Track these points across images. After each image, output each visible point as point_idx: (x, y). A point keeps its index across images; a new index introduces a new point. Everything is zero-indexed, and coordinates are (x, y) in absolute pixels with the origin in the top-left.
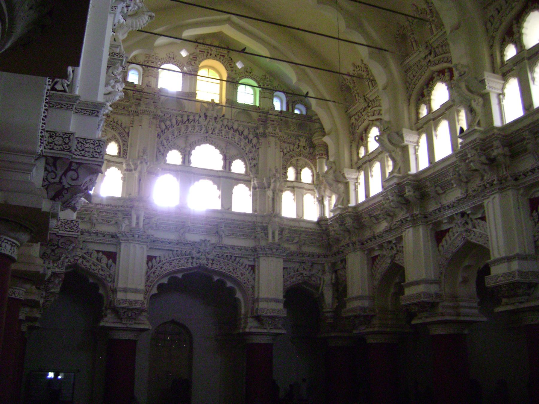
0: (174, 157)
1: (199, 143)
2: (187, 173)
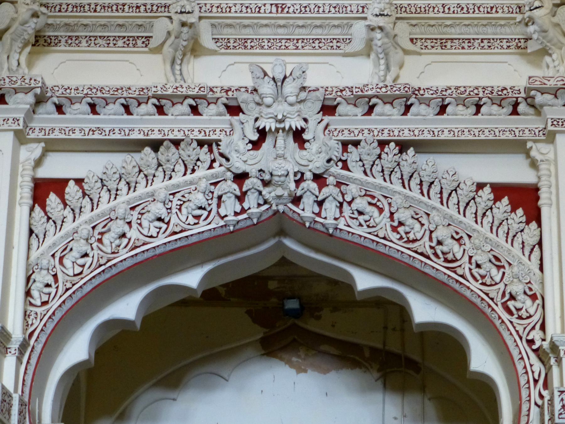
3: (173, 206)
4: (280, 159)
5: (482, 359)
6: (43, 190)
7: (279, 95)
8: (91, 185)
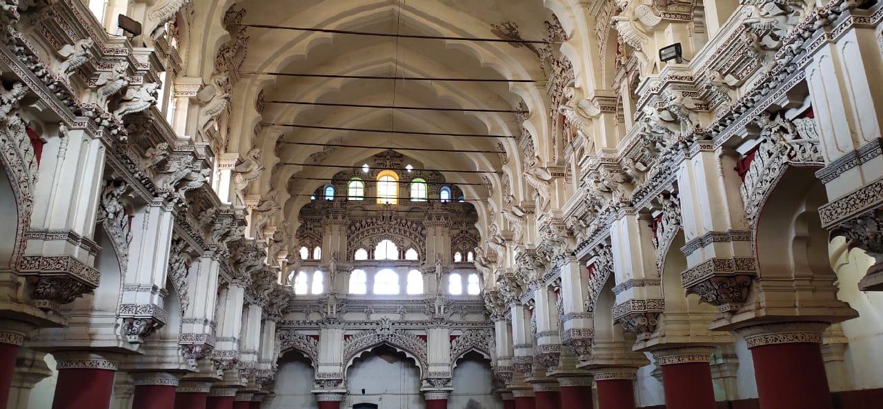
0: (361, 255)
2: (372, 265)
3: (369, 340)
4: (386, 332)
5: (417, 364)
6: (346, 337)
8: (354, 336)
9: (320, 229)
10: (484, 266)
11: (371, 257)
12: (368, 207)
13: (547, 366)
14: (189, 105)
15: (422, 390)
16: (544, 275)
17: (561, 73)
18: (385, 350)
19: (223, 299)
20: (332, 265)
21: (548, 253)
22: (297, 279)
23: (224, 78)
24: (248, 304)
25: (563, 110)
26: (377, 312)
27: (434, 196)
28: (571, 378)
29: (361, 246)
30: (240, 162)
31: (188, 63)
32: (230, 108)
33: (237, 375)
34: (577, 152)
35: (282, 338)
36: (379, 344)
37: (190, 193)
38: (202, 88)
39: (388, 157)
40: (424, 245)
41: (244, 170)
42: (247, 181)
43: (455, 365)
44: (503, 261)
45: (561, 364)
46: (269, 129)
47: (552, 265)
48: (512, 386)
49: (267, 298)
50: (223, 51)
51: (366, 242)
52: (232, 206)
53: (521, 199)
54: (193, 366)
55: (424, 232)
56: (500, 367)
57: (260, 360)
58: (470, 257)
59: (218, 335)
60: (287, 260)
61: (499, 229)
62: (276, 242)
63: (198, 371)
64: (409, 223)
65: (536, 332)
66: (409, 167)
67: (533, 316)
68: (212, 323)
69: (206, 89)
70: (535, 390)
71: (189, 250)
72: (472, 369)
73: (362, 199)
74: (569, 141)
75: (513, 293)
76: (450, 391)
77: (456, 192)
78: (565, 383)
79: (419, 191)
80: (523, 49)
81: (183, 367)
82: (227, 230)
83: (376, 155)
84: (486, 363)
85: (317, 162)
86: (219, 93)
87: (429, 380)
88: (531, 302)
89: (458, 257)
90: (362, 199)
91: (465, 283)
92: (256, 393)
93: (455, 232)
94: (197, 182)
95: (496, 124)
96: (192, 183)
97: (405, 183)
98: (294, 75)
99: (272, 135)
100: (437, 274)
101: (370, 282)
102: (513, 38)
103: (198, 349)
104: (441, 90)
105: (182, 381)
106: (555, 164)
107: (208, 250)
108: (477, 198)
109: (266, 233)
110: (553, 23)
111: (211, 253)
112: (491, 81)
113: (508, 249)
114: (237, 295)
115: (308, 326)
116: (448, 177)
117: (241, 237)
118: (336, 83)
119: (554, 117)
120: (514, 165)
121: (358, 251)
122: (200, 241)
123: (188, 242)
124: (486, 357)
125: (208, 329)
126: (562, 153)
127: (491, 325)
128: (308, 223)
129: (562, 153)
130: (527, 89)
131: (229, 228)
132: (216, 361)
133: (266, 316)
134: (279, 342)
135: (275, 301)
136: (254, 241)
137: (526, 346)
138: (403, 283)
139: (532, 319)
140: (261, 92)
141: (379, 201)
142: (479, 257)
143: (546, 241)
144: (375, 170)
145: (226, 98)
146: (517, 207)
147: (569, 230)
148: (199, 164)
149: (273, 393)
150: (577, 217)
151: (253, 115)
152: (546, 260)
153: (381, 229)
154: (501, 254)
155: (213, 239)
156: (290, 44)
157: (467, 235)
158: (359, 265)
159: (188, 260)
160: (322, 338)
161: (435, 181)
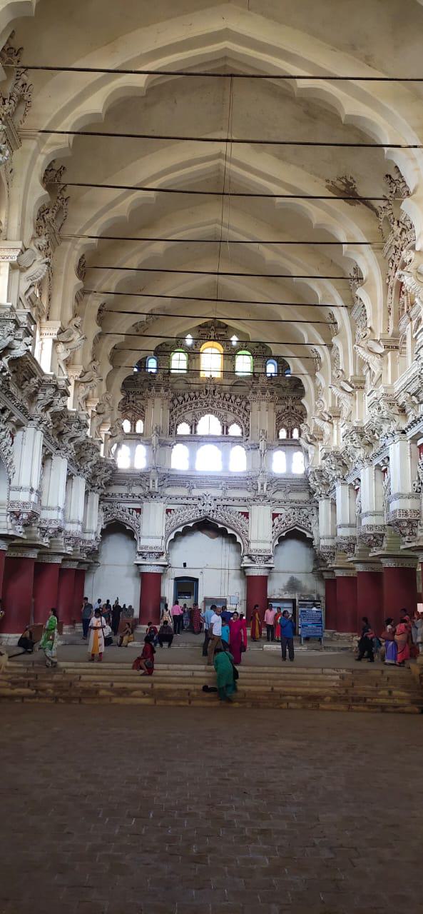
0: (183, 429)
1: (202, 414)
2: (194, 439)
3: (191, 515)
4: (207, 508)
5: (239, 540)
6: (168, 511)
7: (207, 499)
8: (176, 511)
9: (142, 402)
10: (310, 443)
11: (193, 432)
12: (191, 380)
13: (370, 546)
14: (10, 270)
15: (242, 565)
16: (372, 453)
17: (401, 234)
18: (206, 525)
19: (47, 469)
20: (154, 440)
21: (377, 431)
22: (120, 452)
23: (44, 242)
24: (72, 475)
25: (400, 276)
26: (198, 487)
27: (259, 370)
28: (396, 559)
29: (184, 420)
30: (61, 331)
31: (7, 225)
32: (51, 274)
33: (62, 544)
34: (414, 322)
35: (105, 510)
36: (201, 518)
37: (13, 362)
38: (22, 252)
39: (213, 327)
40: (248, 420)
41: (65, 339)
42: (69, 351)
43: (277, 543)
44: (329, 439)
45: (385, 545)
46: (90, 297)
47: (381, 444)
48: (334, 566)
49: (90, 470)
50: (42, 212)
51: (189, 416)
52: (54, 377)
53: (351, 373)
54: (21, 532)
55: (248, 407)
56: (322, 547)
57: (84, 531)
58: (296, 432)
59: (44, 504)
60: (110, 433)
61: (327, 405)
62: (98, 414)
63: (25, 537)
64: (233, 398)
65: (360, 512)
66: (234, 339)
67: (358, 495)
68: (37, 491)
69: (27, 253)
70: (357, 570)
71: (14, 419)
72: (294, 547)
73: (185, 372)
74: (405, 311)
75: (339, 472)
76: (271, 568)
77: (283, 365)
78: (388, 563)
79: (244, 364)
80: (360, 208)
81: (11, 533)
82: (50, 400)
83: (200, 325)
84: (308, 542)
85: (140, 332)
86: (39, 258)
87: (250, 557)
88: (357, 481)
89: (283, 434)
90: (185, 372)
91: (289, 461)
92: (81, 562)
93: (280, 408)
94: (19, 351)
95: (328, 292)
96: (15, 351)
97: (230, 355)
98: (115, 238)
99: (94, 303)
100: (261, 451)
101: (192, 458)
102: (349, 194)
103: (25, 516)
104: (268, 254)
105: (11, 546)
106: (389, 336)
107: (32, 420)
108: (305, 372)
109: (88, 405)
110: (395, 177)
111: (35, 423)
112: (324, 243)
113: (335, 426)
114: (61, 465)
115: (131, 499)
116: (275, 350)
117: (63, 408)
118: (159, 247)
119: (391, 284)
120: (345, 337)
121: (180, 425)
122: (24, 411)
123: (13, 412)
124: (309, 535)
125: (34, 498)
126: (397, 324)
127: (314, 504)
128: (131, 396)
129: (397, 324)
130: (362, 254)
131: (52, 398)
132: (42, 529)
133: (89, 488)
134: (102, 514)
135: (98, 473)
136: (76, 412)
137: (350, 526)
138: (226, 459)
139: (357, 499)
140: (83, 257)
141: (202, 374)
142: (305, 434)
143: (376, 419)
144: (199, 340)
145: (46, 263)
146: (346, 381)
147: (400, 407)
148: (21, 332)
149: (98, 562)
150: (409, 393)
151: (74, 282)
152: (375, 438)
153: (204, 404)
154: (327, 431)
155: (36, 410)
156: (112, 204)
157: (293, 411)
158: (182, 439)
159: (13, 429)
160: (144, 511)
161: (261, 353)
